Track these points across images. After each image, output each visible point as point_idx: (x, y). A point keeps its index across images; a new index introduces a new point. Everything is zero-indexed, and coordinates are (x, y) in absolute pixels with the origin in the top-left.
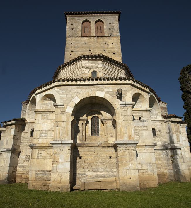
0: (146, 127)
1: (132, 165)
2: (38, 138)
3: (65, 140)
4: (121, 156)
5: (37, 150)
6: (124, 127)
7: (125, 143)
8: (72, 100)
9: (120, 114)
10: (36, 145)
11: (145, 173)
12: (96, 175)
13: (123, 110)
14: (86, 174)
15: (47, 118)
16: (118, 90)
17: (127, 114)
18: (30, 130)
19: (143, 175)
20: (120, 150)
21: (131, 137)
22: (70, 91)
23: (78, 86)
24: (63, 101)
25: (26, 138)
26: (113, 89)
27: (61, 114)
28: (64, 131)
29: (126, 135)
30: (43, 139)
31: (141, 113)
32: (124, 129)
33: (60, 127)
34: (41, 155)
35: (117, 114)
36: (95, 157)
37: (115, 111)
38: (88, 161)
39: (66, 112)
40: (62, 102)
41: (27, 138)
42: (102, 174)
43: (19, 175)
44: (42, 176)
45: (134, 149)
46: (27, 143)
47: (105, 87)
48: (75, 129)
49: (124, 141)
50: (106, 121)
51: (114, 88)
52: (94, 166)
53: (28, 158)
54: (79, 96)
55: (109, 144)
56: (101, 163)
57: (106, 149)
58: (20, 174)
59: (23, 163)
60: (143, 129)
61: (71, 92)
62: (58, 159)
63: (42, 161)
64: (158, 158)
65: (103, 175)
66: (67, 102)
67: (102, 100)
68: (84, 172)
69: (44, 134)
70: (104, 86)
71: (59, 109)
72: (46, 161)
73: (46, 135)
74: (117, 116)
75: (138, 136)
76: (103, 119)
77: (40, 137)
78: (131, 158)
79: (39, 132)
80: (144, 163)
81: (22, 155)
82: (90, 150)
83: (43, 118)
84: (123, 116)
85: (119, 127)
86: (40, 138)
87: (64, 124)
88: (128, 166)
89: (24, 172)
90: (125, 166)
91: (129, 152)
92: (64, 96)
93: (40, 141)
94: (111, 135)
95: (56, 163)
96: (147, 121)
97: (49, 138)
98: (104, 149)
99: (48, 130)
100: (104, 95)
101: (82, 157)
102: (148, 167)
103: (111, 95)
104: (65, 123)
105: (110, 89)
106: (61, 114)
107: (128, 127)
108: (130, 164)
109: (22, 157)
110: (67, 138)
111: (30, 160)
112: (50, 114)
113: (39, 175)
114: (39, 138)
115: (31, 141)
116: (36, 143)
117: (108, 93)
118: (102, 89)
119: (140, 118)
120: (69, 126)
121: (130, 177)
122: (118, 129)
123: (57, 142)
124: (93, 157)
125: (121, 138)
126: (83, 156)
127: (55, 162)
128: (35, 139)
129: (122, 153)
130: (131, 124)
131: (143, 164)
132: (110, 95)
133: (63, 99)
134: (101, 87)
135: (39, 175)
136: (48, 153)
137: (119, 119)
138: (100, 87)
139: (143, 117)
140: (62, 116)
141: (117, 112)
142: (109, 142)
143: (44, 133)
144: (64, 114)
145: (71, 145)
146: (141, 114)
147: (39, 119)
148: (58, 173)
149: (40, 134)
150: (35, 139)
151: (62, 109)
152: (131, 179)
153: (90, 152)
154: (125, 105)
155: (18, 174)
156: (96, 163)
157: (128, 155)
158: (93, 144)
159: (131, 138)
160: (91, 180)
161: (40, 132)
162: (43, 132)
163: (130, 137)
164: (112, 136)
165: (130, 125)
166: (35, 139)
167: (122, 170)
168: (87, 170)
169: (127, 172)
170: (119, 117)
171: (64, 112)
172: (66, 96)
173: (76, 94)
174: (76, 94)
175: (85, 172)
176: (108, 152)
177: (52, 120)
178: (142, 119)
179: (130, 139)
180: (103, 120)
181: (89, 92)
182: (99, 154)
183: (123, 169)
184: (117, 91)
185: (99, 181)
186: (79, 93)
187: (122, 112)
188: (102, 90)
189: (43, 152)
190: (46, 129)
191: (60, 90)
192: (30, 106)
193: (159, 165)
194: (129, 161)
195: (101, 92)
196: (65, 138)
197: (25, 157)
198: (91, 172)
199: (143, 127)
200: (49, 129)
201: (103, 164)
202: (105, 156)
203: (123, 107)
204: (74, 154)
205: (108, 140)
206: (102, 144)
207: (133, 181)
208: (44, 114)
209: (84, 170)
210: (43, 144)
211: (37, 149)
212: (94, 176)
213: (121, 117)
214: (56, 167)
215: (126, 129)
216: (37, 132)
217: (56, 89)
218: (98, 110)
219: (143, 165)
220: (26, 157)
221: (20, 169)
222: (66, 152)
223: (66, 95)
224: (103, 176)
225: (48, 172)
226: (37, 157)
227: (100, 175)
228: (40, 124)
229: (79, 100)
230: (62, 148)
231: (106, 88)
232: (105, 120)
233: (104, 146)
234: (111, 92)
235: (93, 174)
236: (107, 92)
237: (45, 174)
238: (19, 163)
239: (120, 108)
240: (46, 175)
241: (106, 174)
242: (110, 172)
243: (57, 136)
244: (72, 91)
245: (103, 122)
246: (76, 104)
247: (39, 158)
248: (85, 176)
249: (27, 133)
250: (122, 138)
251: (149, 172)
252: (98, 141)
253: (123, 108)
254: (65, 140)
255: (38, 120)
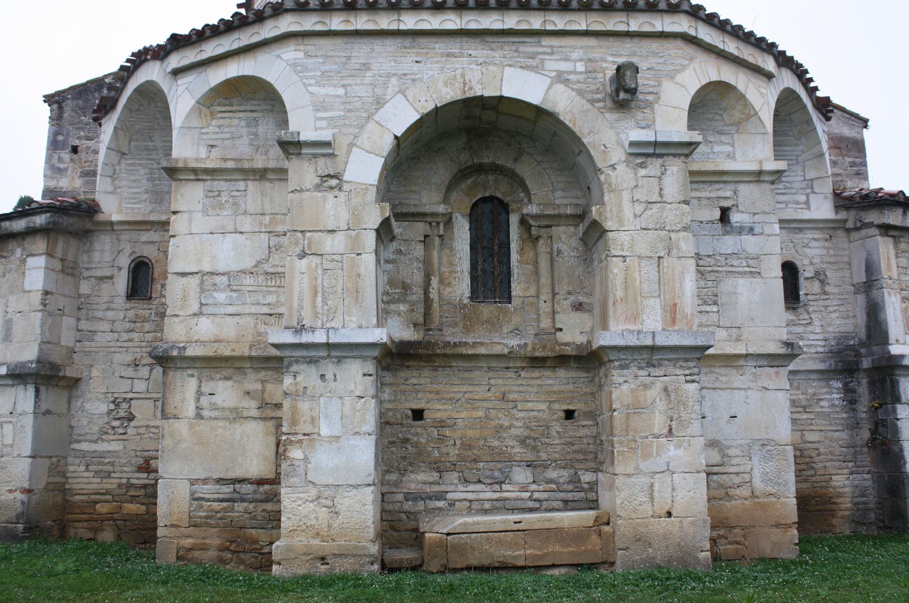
0: (751, 262)
1: (680, 452)
2: (192, 312)
3: (343, 327)
4: (628, 407)
5: (193, 376)
6: (644, 263)
7: (649, 342)
8: (377, 117)
9: (626, 197)
10: (184, 348)
11: (737, 492)
12: (497, 500)
13: (642, 172)
14: (449, 496)
15: (235, 204)
16: (618, 69)
17: (661, 196)
18: (125, 262)
19: (729, 497)
20: (621, 380)
21: (678, 316)
22: (366, 67)
23: (407, 42)
24: (332, 118)
25: (104, 307)
26: (590, 60)
27: (318, 187)
28: (341, 282)
29: (652, 301)
30: (217, 320)
31: (732, 186)
32: (644, 271)
33: (317, 260)
34: (214, 399)
35: (612, 196)
36: (493, 413)
37: (602, 178)
38: (459, 434)
39: (346, 177)
40: (324, 124)
41: (108, 309)
42: (528, 494)
43: (82, 501)
44: (225, 504)
45: (691, 375)
46: (110, 336)
47: (549, 50)
48: (389, 267)
49: (641, 336)
50: (550, 226)
51: (596, 55)
52: (489, 459)
53: (122, 414)
54: (410, 94)
55: (566, 344)
56: (523, 442)
57: (548, 373)
58: (83, 497)
59: (96, 441)
60: (739, 273)
61: (368, 74)
62: (313, 421)
63: (220, 431)
64: (804, 416)
65: (530, 499)
66: (351, 126)
67: (531, 115)
68: (436, 488)
69: (223, 290)
70: (547, 41)
71: (306, 164)
72: (238, 431)
73: (234, 295)
74: (608, 208)
75: (708, 308)
76: (536, 217)
77: (202, 304)
78: (675, 417)
79: (194, 281)
80: (733, 443)
81: (89, 396)
82: (466, 375)
83: (213, 208)
84: (639, 208)
85: (621, 264)
86: (205, 310)
87: (334, 244)
88: (658, 454)
89: (109, 486)
90: (646, 456)
91: (666, 389)
92: (331, 91)
93: (205, 328)
94: (572, 298)
95: (300, 442)
96: (757, 230)
97: (247, 311)
98: (536, 373)
99: (243, 272)
100: (544, 93)
101: (426, 414)
102: (755, 459)
103: (580, 93)
104: (340, 238)
105: (575, 61)
106: (318, 187)
107: (665, 262)
108: (672, 448)
109: (88, 406)
110: (354, 319)
111: (132, 424)
112: (250, 183)
113: (208, 500)
114: (195, 315)
115: (132, 325)
116: (184, 338)
117: (566, 82)
118: (533, 56)
119: (725, 213)
120: (363, 256)
121: (667, 508)
122: (615, 271)
123: (306, 338)
124: (481, 414)
125: (627, 320)
126: (429, 406)
127: (301, 437)
128: (177, 316)
129: (633, 391)
130: (679, 249)
131: (729, 447)
132: (574, 94)
133: (326, 109)
134: (529, 47)
135: (208, 500)
136: (248, 393)
137: (620, 221)
138: (522, 49)
139: (741, 208)
140: (325, 199)
141: (610, 185)
142: (562, 337)
143: (222, 286)
144: (336, 192)
145: (376, 353)
146: (728, 194)
147: (190, 212)
148: (314, 492)
149: (203, 291)
150: (176, 320)
151: (324, 166)
152: (672, 518)
153: (465, 389)
154: (651, 151)
155: (77, 498)
156: (496, 443)
157: (661, 405)
158: (481, 344)
159: (677, 321)
160: (475, 523)
161: (202, 282)
162: (218, 279)
163: (672, 313)
164: (581, 304)
165: (674, 251)
166: (177, 316)
167: (629, 475)
168: (454, 475)
169: (652, 485)
170: (620, 211)
171: (334, 182)
172: (341, 91)
173: (394, 81)
174: (394, 81)
175: (443, 488)
176: (555, 389)
177: (262, 218)
178: (736, 218)
179: (674, 322)
180: (532, 222)
181: (463, 75)
182: (511, 397)
183: (638, 472)
184: (611, 72)
185: (517, 527)
186: (414, 80)
187: (636, 186)
188: (531, 62)
189: (220, 382)
190: (235, 267)
191: (310, 61)
192: (120, 132)
193: (806, 453)
194: (665, 431)
195: (526, 73)
196: (347, 318)
197: (103, 408)
198: (471, 487)
199: (735, 263)
200: (248, 264)
201: (535, 449)
202: (543, 406)
203: (639, 161)
204: (386, 396)
205: (558, 326)
206: (529, 348)
207: (681, 527)
208: (216, 183)
209: (436, 475)
210: (222, 345)
211: (190, 372)
212: (487, 506)
213: (628, 210)
214: (306, 459)
215: (654, 275)
216: (185, 280)
217: (290, 53)
218: (509, 164)
219: (731, 452)
220: (112, 406)
221: (82, 468)
222: (352, 387)
223: (344, 86)
224: (531, 504)
225: (254, 487)
226: (191, 411)
227: (516, 499)
228: (197, 237)
229: (416, 117)
230: (330, 369)
231: (552, 53)
232: (543, 223)
233: (537, 354)
234: (581, 77)
235: (482, 496)
236: (560, 73)
237: (236, 496)
238: (79, 442)
239: (627, 162)
240: (243, 500)
241: (545, 495)
242: (565, 487)
243: (301, 307)
244: (375, 66)
245: (534, 231)
246: (396, 137)
247: (206, 413)
248: (441, 504)
249: (111, 278)
250: (635, 317)
251: (758, 483)
252: (505, 331)
253: (642, 165)
254: (343, 327)
255: (185, 216)
